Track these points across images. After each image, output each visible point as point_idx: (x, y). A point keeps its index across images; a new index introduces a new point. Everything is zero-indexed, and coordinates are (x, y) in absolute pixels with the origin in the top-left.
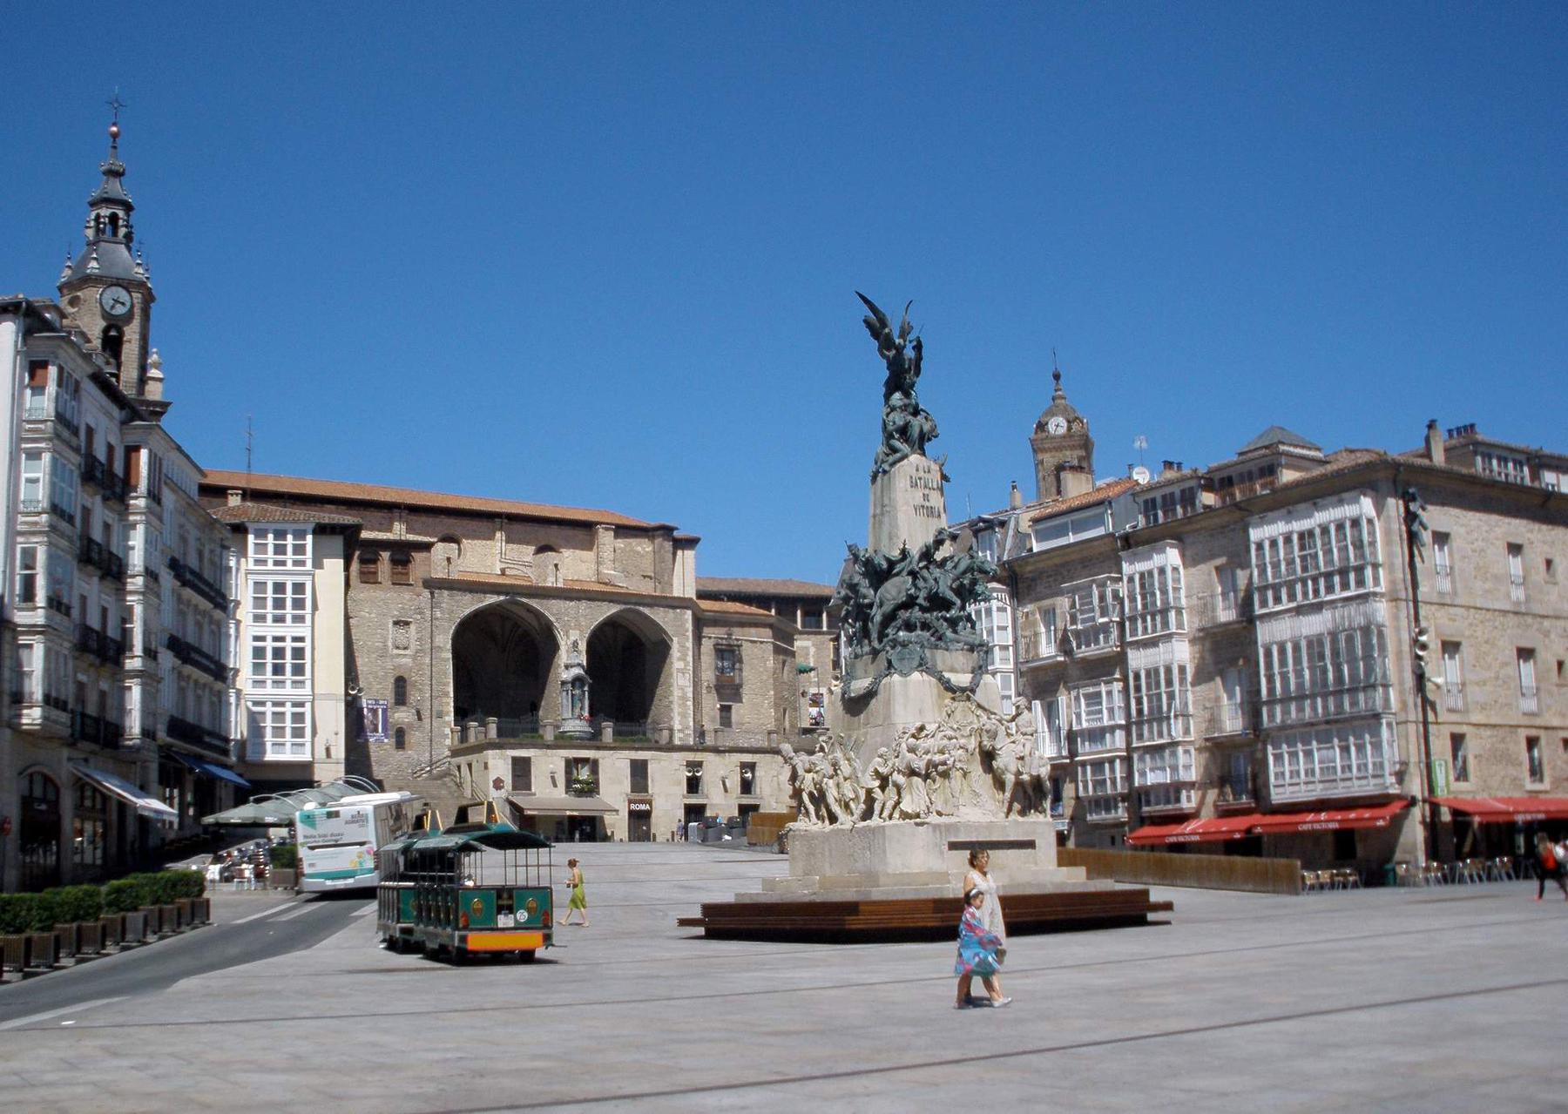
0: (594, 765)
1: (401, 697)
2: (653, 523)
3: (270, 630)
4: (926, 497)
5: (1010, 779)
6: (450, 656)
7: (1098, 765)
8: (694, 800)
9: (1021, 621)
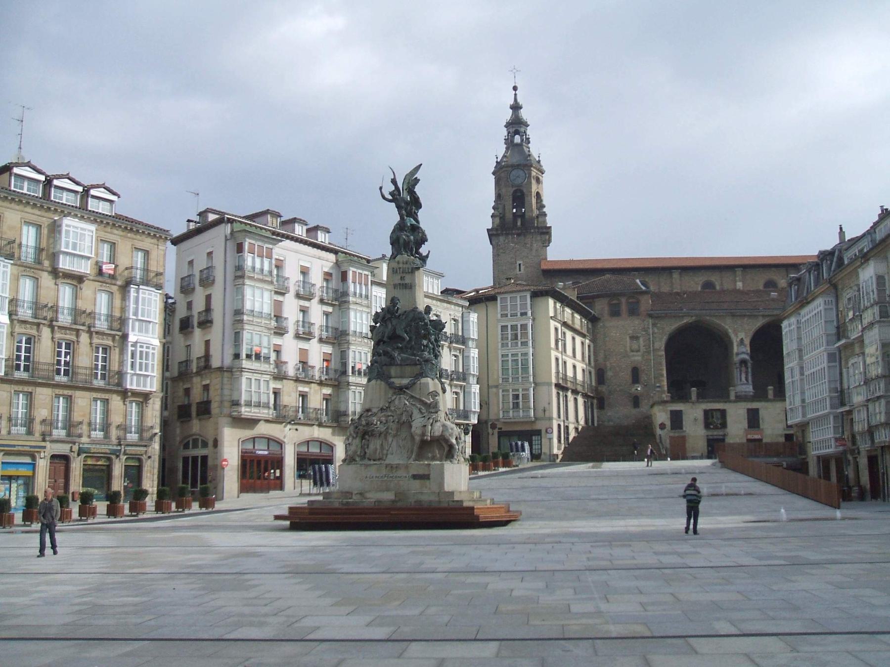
0: (723, 413)
1: (636, 379)
3: (520, 350)
4: (402, 278)
5: (417, 439)
6: (663, 353)
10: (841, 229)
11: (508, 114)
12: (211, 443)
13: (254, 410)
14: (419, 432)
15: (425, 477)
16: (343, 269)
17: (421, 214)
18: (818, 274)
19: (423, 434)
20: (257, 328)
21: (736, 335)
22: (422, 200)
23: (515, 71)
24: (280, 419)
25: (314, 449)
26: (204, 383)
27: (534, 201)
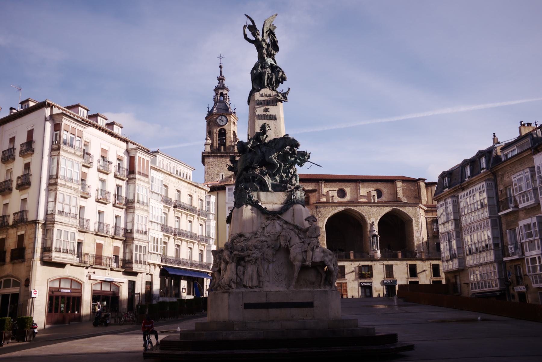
0: (370, 268)
2: (417, 178)
5: (297, 264)
7: (533, 260)
8: (413, 280)
9: (499, 194)
10: (494, 136)
11: (216, 83)
12: (23, 283)
13: (62, 255)
14: (300, 257)
15: (310, 305)
16: (132, 154)
17: (278, 56)
18: (473, 168)
19: (304, 260)
20: (69, 191)
21: (369, 219)
22: (279, 45)
23: (221, 58)
24: (82, 264)
25: (106, 288)
26: (19, 233)
27: (232, 136)
